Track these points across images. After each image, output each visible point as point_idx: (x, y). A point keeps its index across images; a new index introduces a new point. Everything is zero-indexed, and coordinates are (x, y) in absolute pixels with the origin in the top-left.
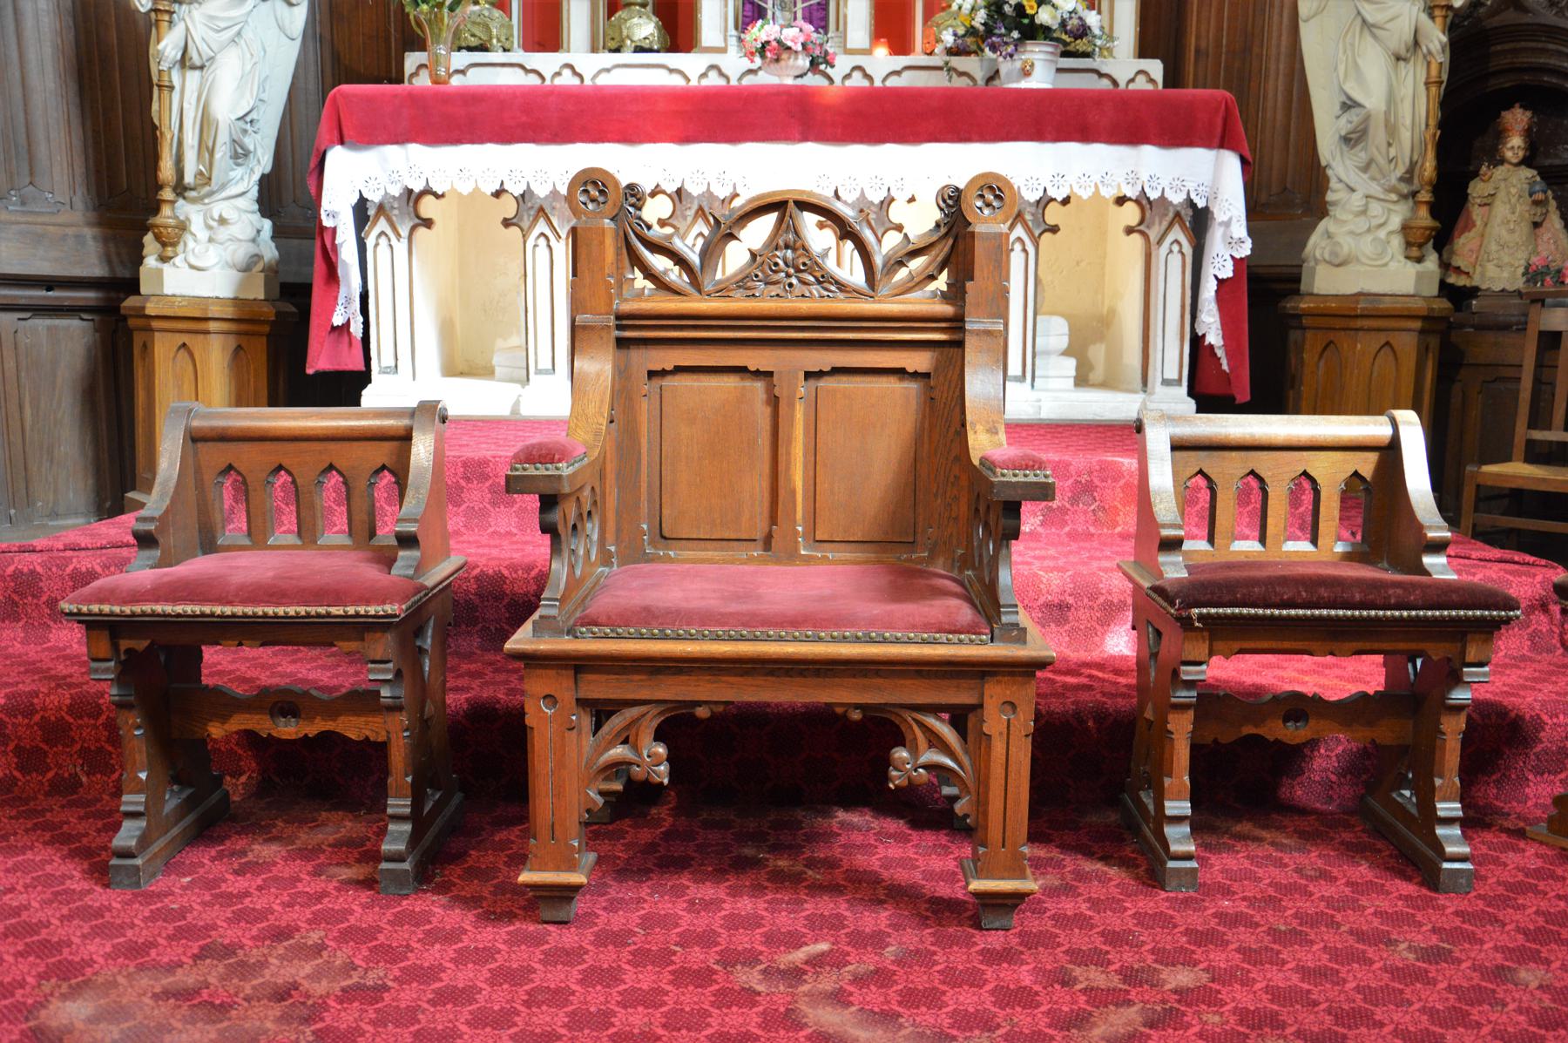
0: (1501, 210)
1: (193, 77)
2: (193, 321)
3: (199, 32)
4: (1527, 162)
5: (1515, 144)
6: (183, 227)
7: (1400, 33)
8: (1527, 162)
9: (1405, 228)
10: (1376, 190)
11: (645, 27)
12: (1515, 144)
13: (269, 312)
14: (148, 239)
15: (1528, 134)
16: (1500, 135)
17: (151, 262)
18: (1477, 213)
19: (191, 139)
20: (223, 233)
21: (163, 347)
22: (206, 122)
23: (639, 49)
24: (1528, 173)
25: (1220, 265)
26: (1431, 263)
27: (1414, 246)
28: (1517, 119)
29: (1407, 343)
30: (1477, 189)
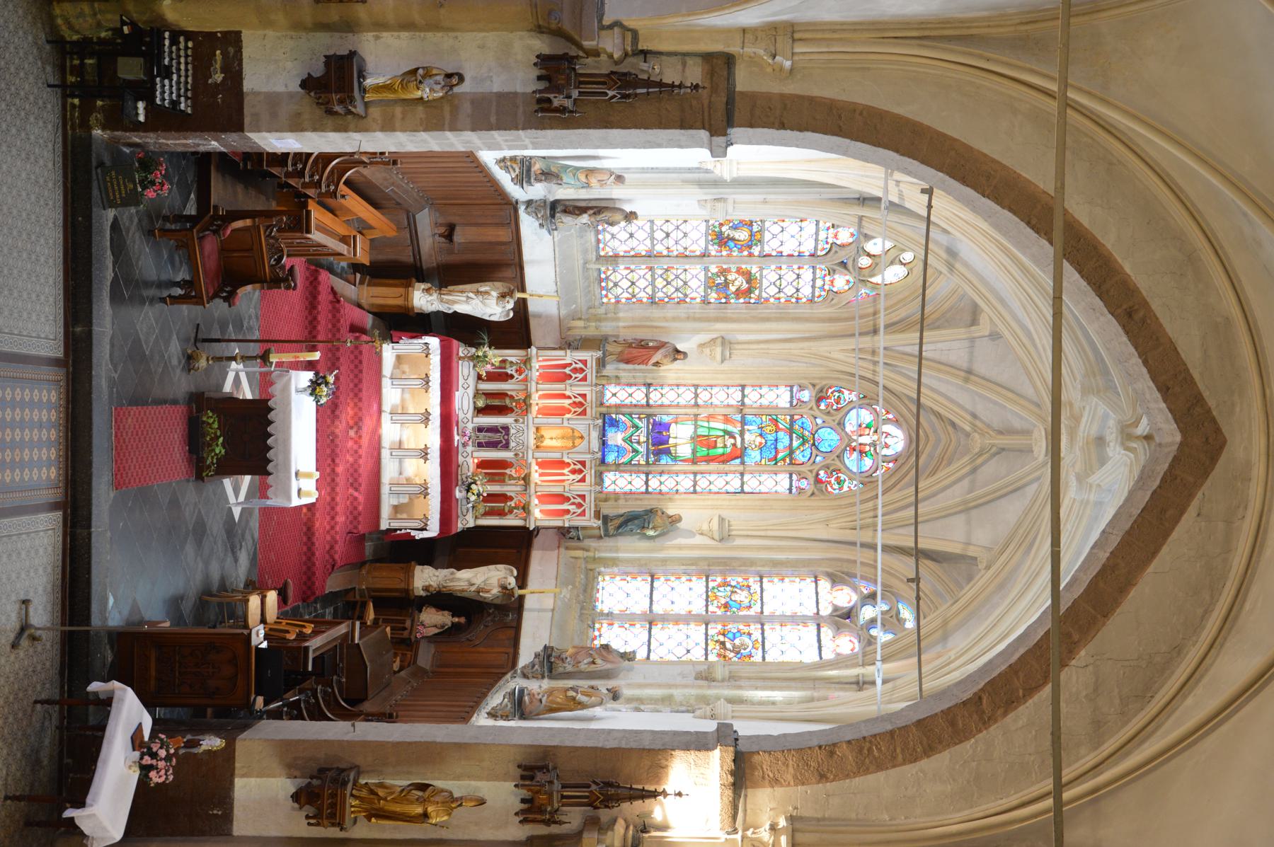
0: (440, 617)
1: (464, 299)
2: (407, 297)
3: (474, 302)
4: (453, 623)
5: (456, 620)
6: (431, 295)
7: (474, 581)
8: (453, 623)
9: (430, 586)
10: (440, 579)
11: (481, 404)
12: (456, 620)
13: (411, 314)
14: (429, 285)
15: (459, 623)
16: (459, 616)
17: (423, 286)
18: (440, 613)
19: (450, 298)
20: (429, 304)
21: (401, 290)
22: (454, 302)
23: (474, 403)
24: (450, 624)
25: (413, 533)
26: (422, 593)
27: (426, 589)
28: (463, 620)
29: (402, 586)
30: (446, 613)
